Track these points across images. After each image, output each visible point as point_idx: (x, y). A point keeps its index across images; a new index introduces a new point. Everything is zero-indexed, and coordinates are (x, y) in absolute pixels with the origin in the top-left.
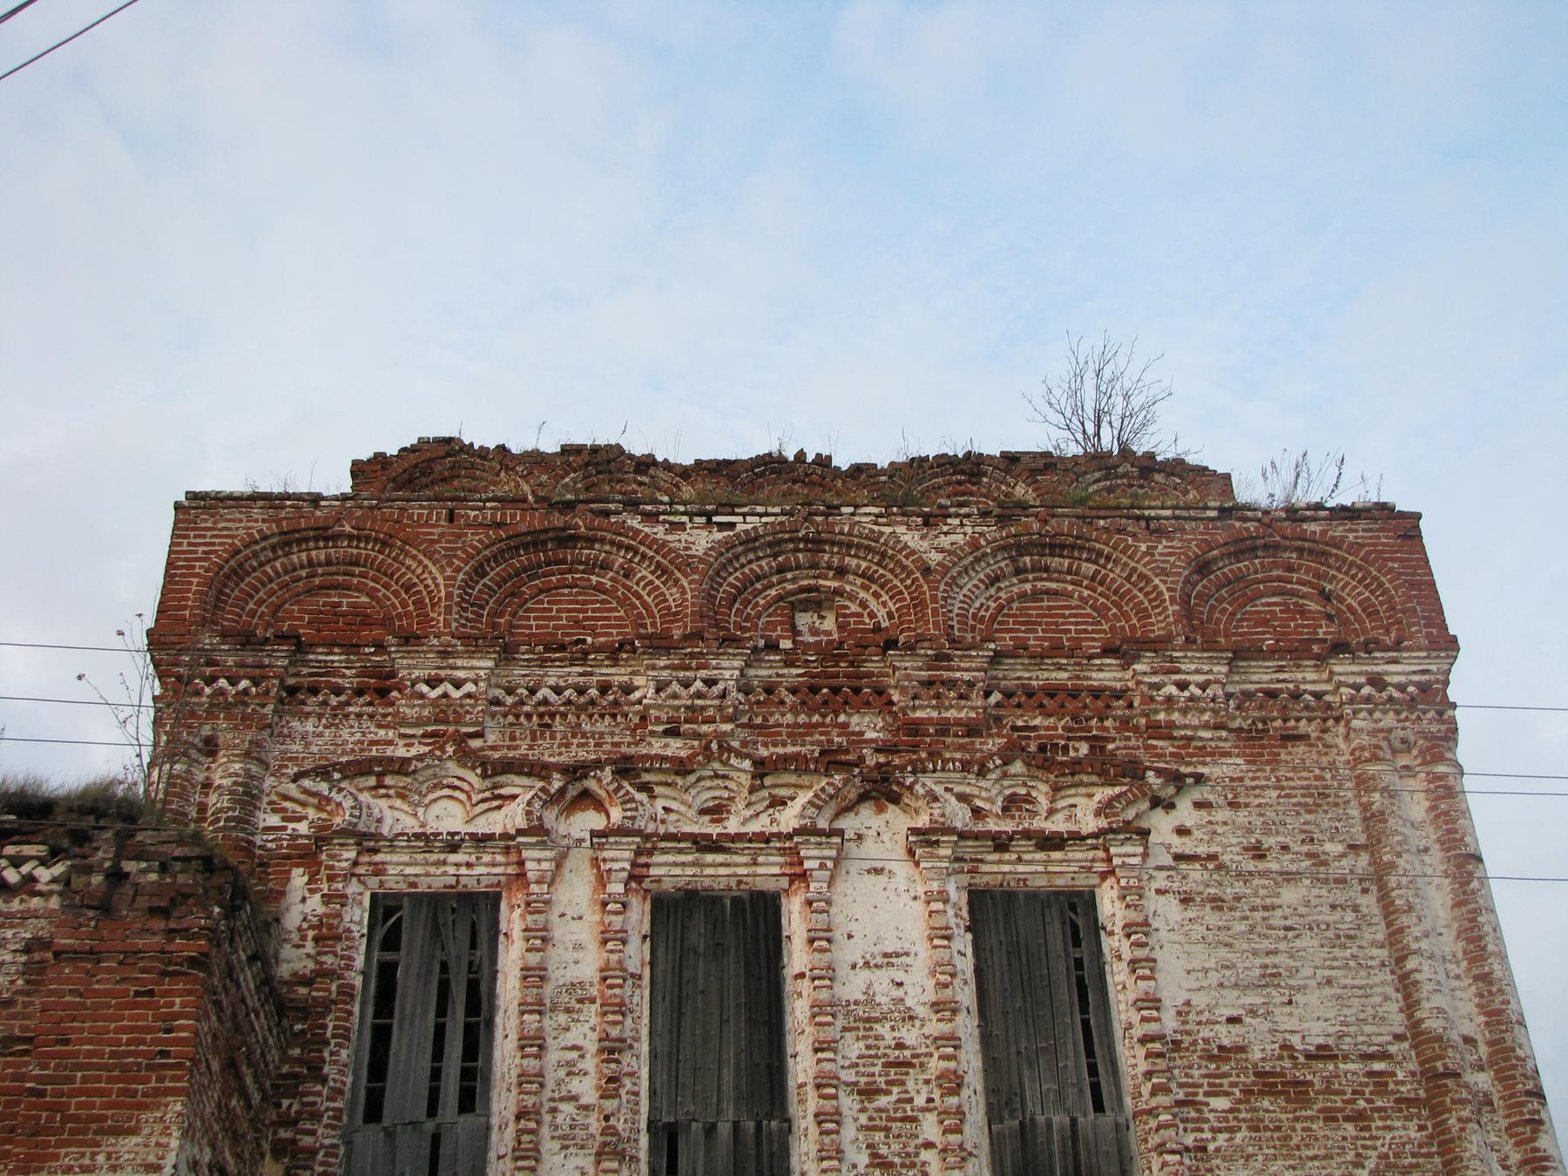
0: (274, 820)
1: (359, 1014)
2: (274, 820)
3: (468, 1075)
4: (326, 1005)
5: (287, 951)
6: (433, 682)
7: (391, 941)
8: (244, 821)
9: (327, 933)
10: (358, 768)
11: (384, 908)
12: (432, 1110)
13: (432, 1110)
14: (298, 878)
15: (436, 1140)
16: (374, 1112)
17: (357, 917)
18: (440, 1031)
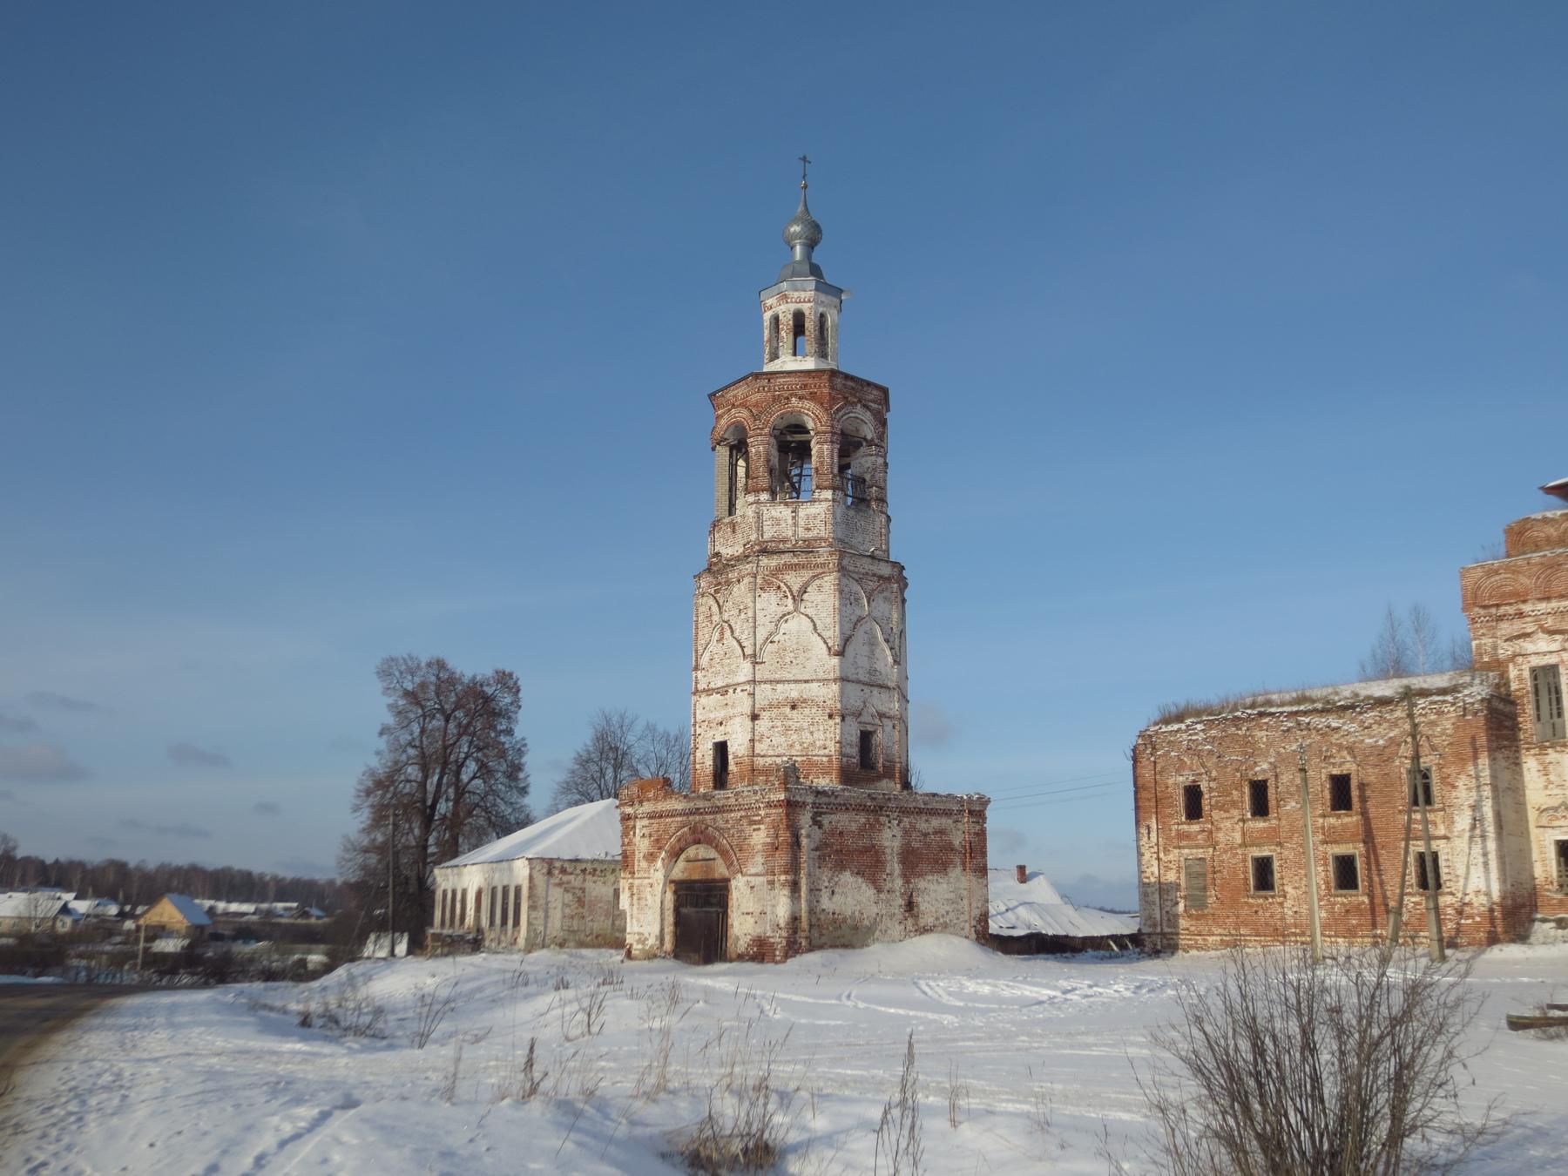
0: (1502, 651)
1: (1531, 697)
2: (1502, 651)
3: (1558, 709)
4: (1523, 696)
5: (1512, 684)
6: (1533, 611)
7: (1535, 678)
8: (1496, 654)
9: (1520, 678)
10: (1518, 637)
11: (1533, 670)
12: (1551, 717)
13: (1551, 717)
14: (1511, 666)
15: (1554, 724)
16: (1539, 719)
17: (1526, 674)
18: (1550, 699)
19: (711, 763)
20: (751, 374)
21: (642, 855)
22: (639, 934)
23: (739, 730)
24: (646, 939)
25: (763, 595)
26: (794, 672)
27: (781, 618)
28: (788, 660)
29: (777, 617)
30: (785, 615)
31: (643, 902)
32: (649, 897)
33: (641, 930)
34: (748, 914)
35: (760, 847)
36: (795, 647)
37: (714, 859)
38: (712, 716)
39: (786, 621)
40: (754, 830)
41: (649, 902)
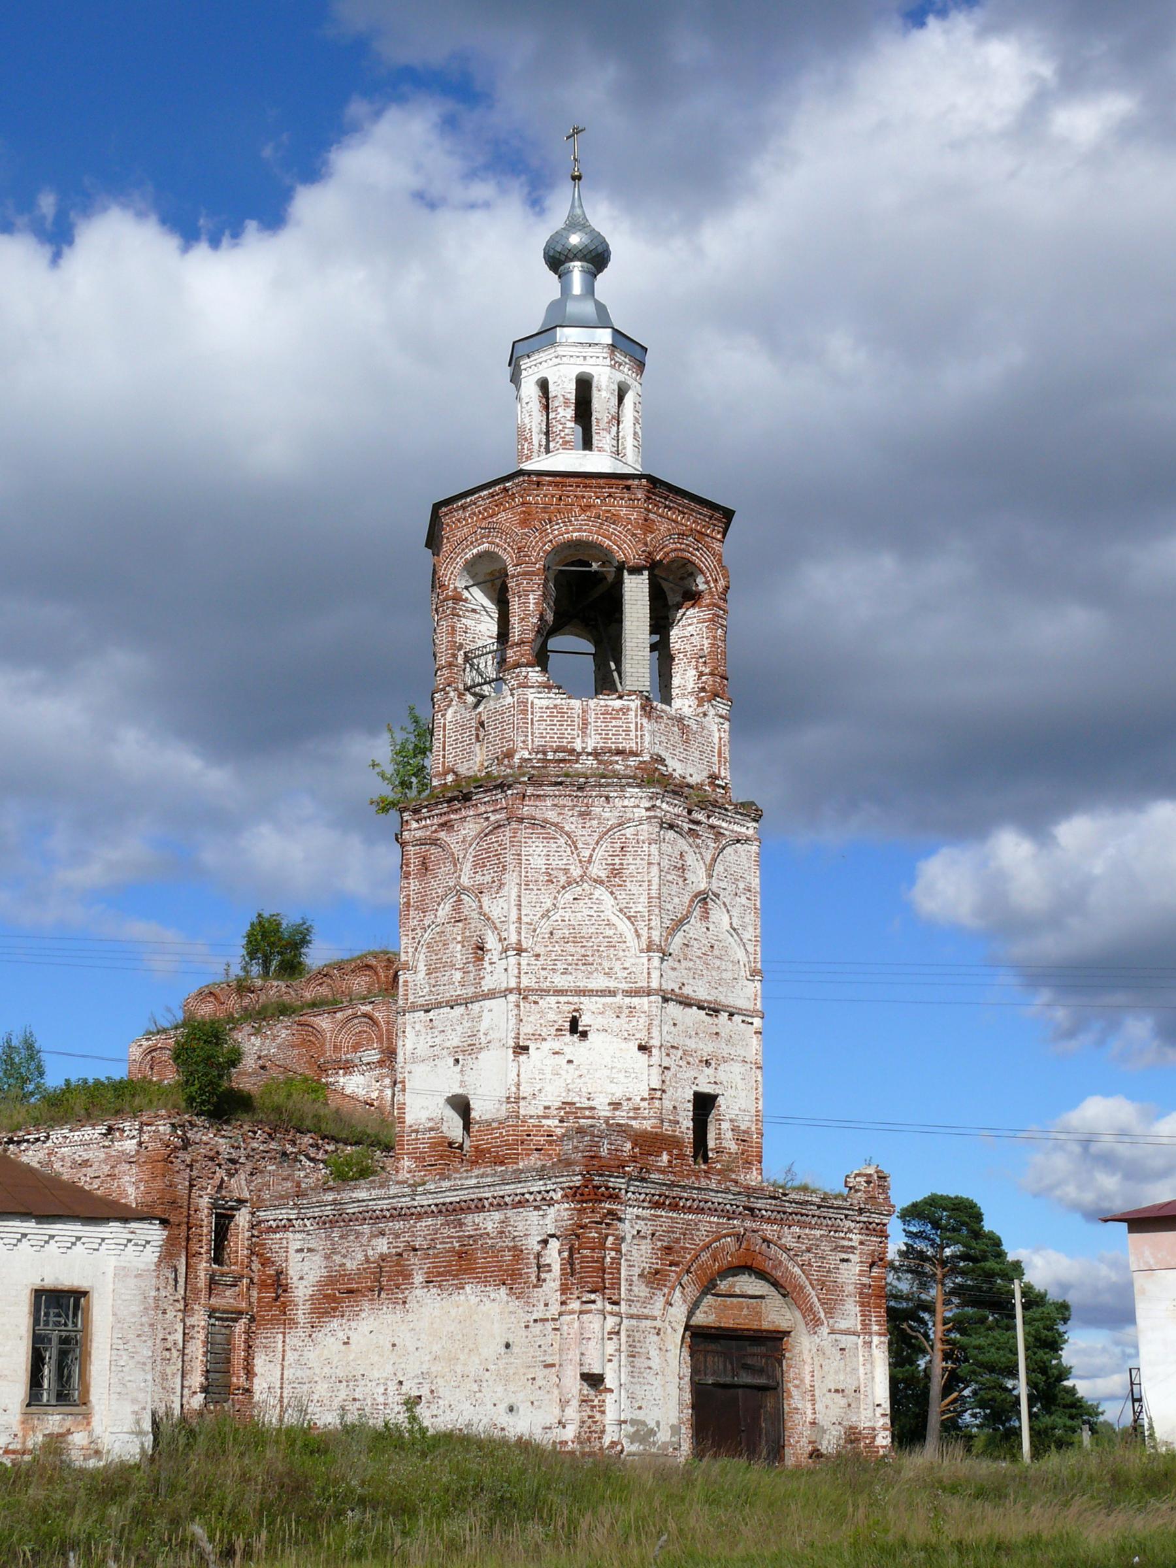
19: (691, 1125)
20: (649, 478)
21: (636, 1271)
22: (634, 1422)
23: (741, 1085)
24: (652, 1433)
31: (640, 1362)
32: (654, 1353)
33: (640, 1415)
34: (837, 1391)
35: (850, 1289)
37: (762, 1297)
38: (691, 1044)
40: (843, 1260)
41: (655, 1363)
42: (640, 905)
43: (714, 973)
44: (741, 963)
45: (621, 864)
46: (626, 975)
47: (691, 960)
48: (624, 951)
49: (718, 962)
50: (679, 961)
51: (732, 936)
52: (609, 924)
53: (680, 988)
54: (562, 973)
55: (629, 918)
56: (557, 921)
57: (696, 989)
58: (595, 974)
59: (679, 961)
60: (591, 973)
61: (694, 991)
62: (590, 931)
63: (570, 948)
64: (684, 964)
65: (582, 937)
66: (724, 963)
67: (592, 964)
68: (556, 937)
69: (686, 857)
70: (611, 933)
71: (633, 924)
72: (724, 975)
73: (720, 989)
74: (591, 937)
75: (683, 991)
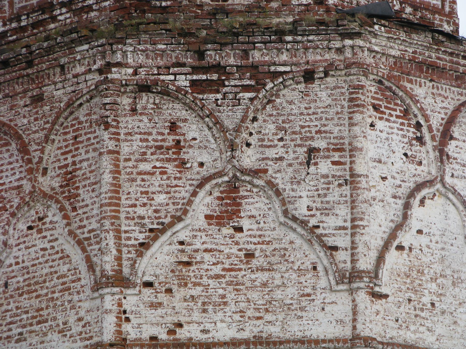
25: (380, 125)
26: (440, 329)
27: (412, 195)
28: (426, 300)
29: (404, 191)
30: (419, 187)
36: (437, 268)
39: (422, 202)
42: (93, 220)
43: (254, 295)
44: (320, 268)
45: (74, 163)
46: (80, 329)
47: (195, 284)
48: (78, 293)
49: (262, 277)
50: (169, 291)
51: (294, 230)
52: (65, 257)
53: (171, 332)
54: (17, 341)
55: (79, 243)
56: (11, 265)
57: (208, 326)
58: (50, 336)
59: (169, 291)
60: (45, 334)
61: (205, 331)
62: (45, 271)
63: (25, 302)
64: (179, 293)
65: (37, 283)
66: (278, 276)
67: (46, 321)
68: (11, 288)
69: (184, 127)
70: (64, 269)
71: (84, 250)
72: (278, 294)
73: (269, 317)
74: (45, 281)
75: (178, 336)
